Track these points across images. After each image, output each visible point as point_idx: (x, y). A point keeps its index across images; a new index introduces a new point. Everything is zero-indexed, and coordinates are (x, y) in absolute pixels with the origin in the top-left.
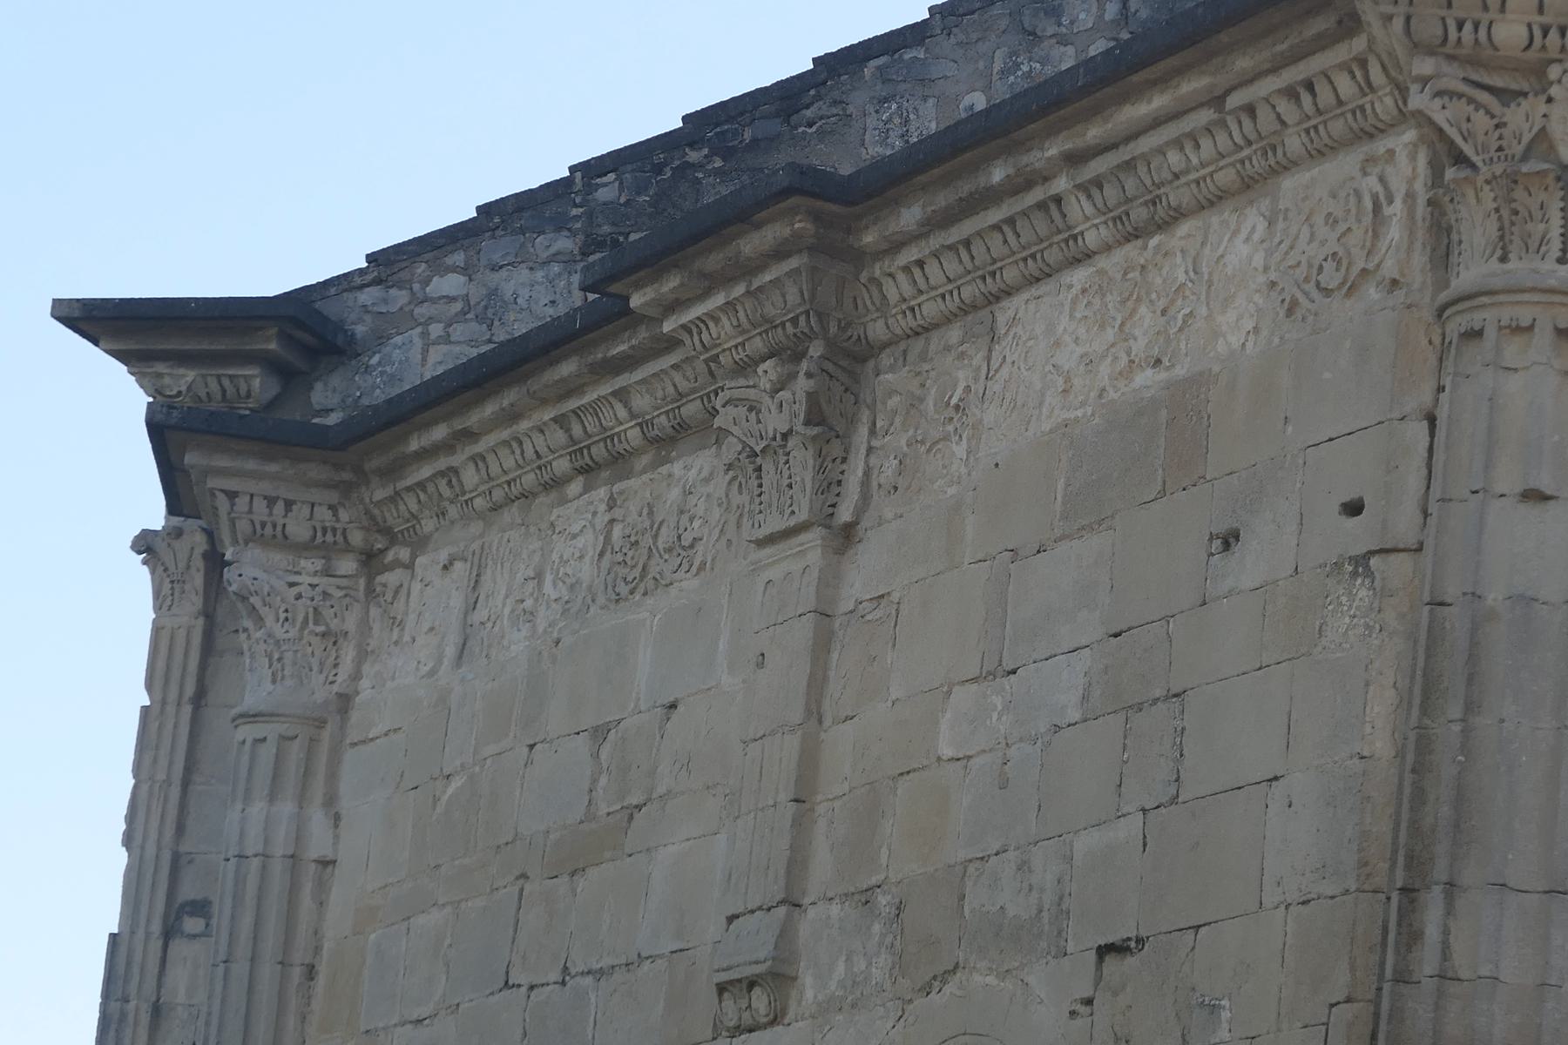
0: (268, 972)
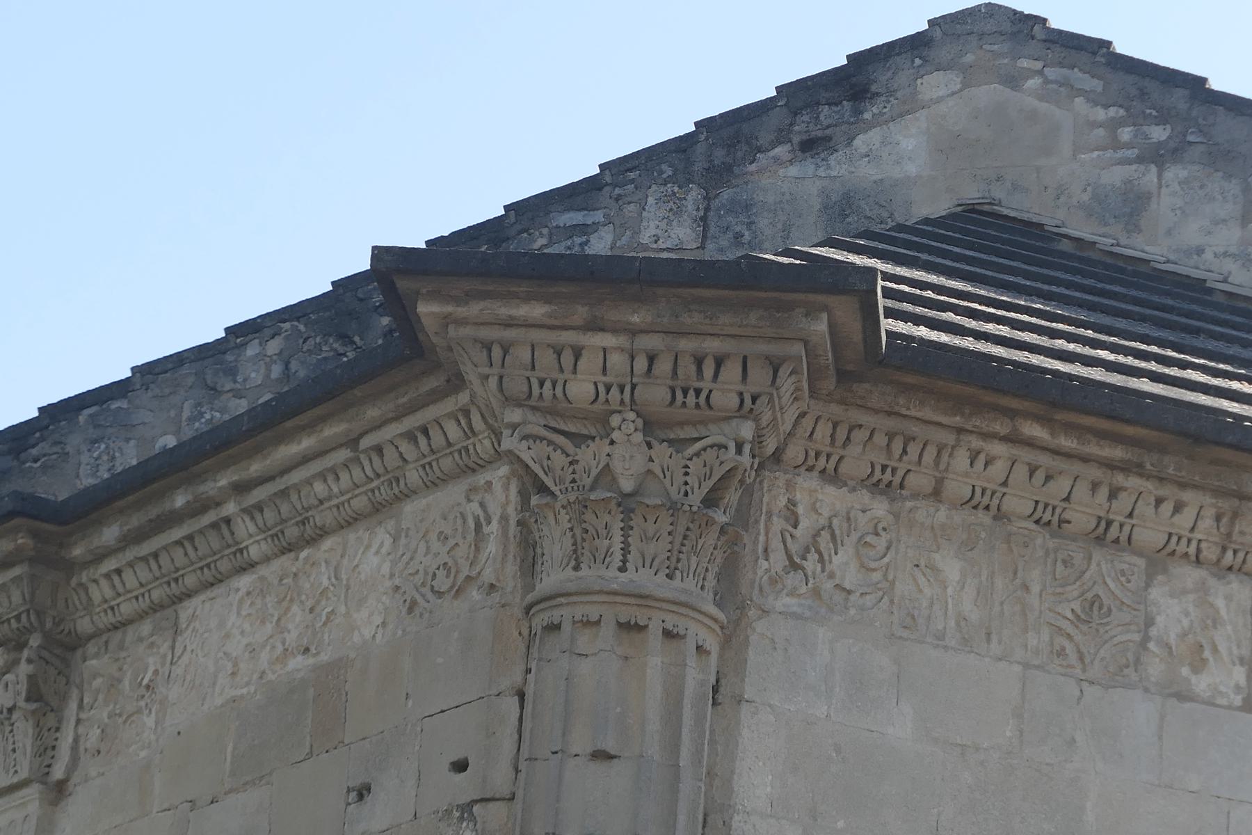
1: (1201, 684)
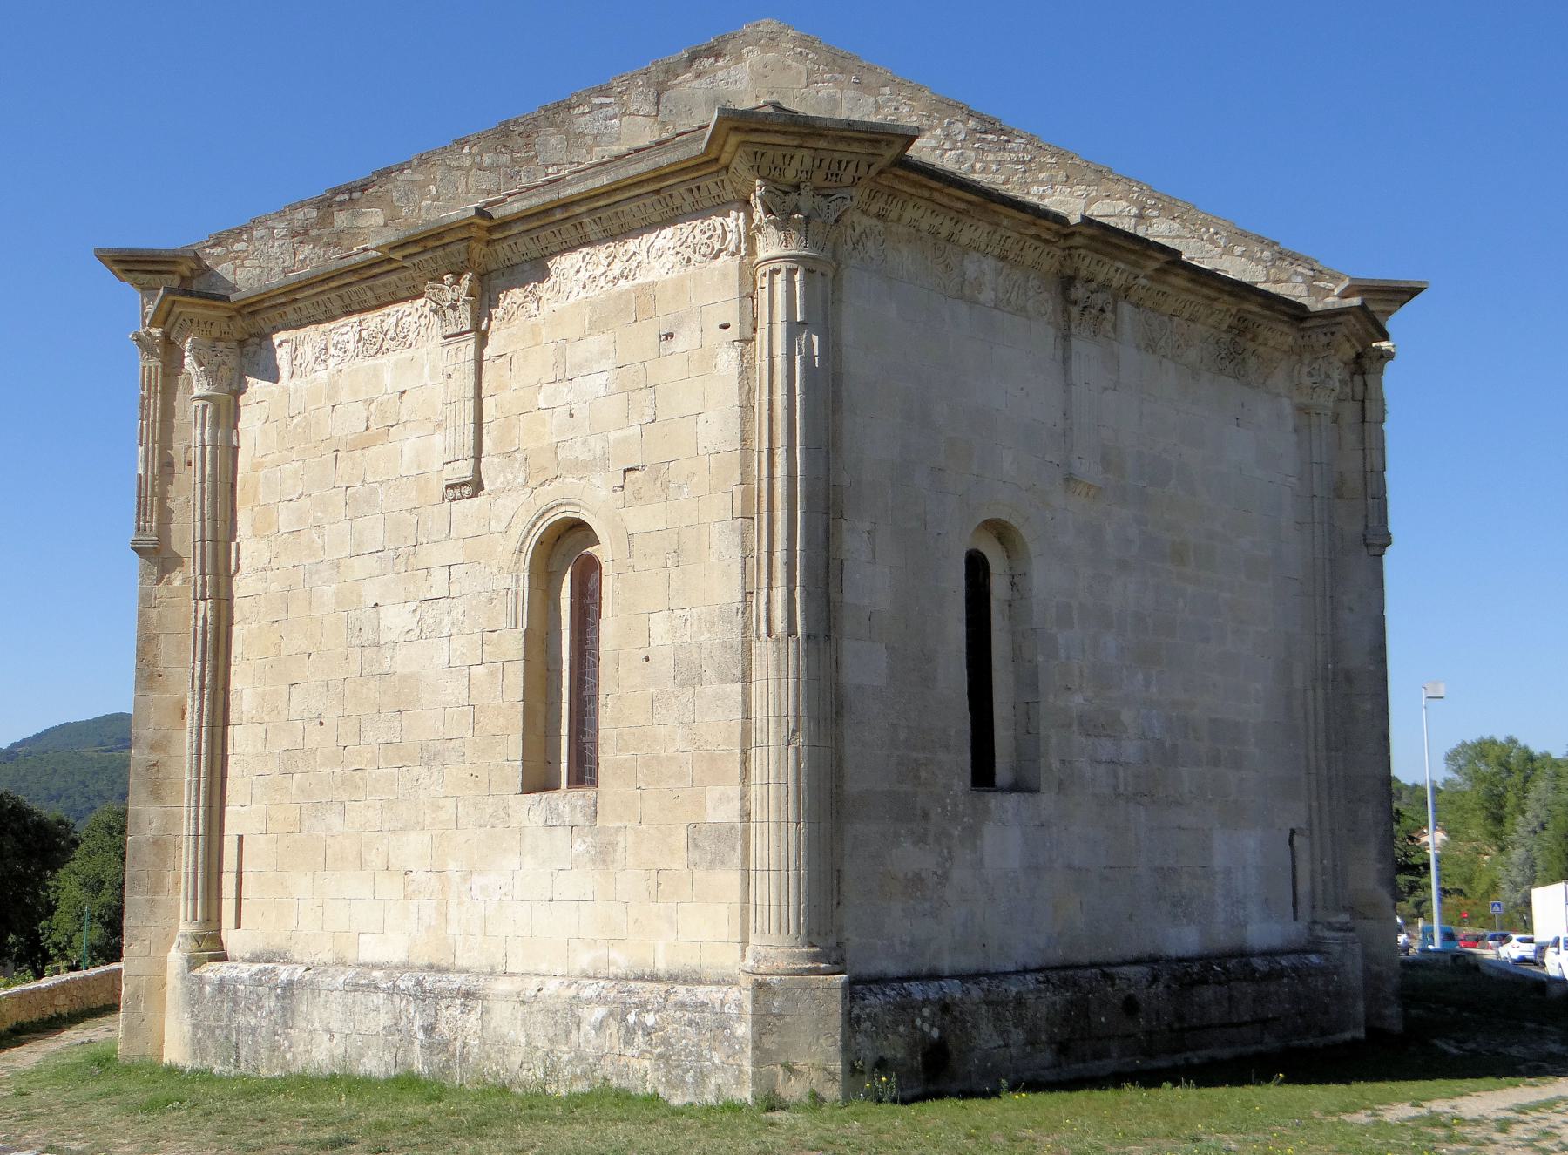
1: (982, 298)
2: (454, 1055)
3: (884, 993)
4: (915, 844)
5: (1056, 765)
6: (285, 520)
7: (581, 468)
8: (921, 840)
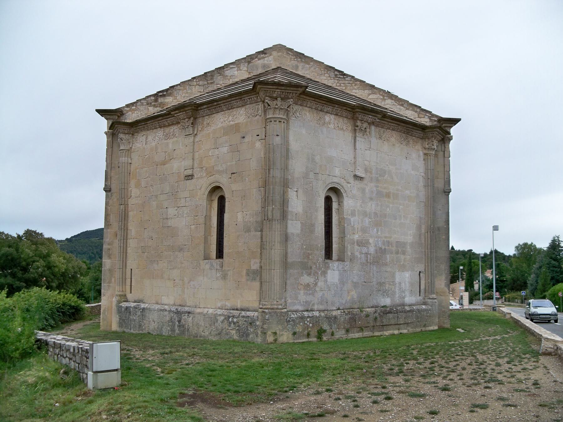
0: (126, 174)
2: (186, 328)
3: (297, 315)
4: (308, 275)
5: (349, 254)
6: (143, 184)
7: (219, 172)
8: (309, 274)
